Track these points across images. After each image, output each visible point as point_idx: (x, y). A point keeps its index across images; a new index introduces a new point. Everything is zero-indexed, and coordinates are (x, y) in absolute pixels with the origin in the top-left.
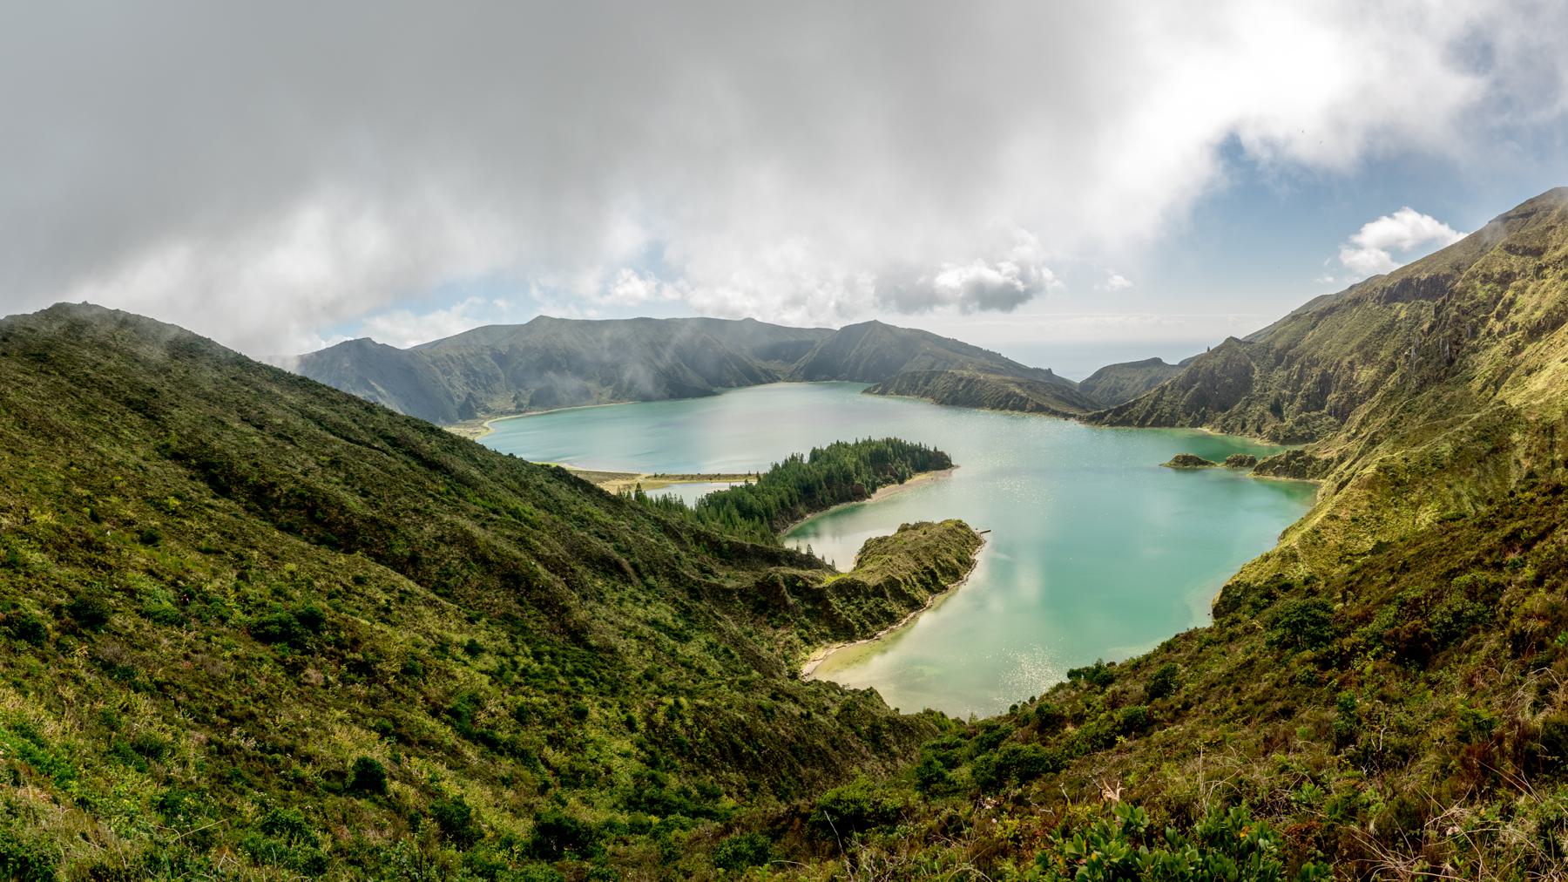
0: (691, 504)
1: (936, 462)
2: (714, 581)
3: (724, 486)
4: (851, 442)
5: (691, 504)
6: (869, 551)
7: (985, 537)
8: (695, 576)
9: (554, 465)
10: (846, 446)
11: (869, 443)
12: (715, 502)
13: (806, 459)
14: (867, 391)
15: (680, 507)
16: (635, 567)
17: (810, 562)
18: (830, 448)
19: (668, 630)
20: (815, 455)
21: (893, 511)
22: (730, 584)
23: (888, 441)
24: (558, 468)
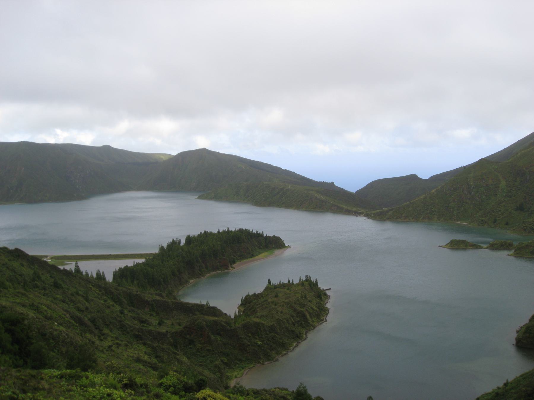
0: (109, 278)
1: (274, 244)
2: (152, 328)
3: (130, 263)
4: (215, 231)
5: (109, 278)
6: (249, 303)
7: (328, 292)
8: (137, 325)
9: (12, 248)
10: (211, 234)
11: (228, 232)
12: (122, 275)
13: (183, 242)
14: (200, 197)
15: (100, 277)
16: (93, 321)
17: (214, 311)
18: (200, 235)
19: (145, 363)
20: (189, 240)
21: (256, 277)
22: (163, 330)
23: (241, 230)
24: (17, 250)
